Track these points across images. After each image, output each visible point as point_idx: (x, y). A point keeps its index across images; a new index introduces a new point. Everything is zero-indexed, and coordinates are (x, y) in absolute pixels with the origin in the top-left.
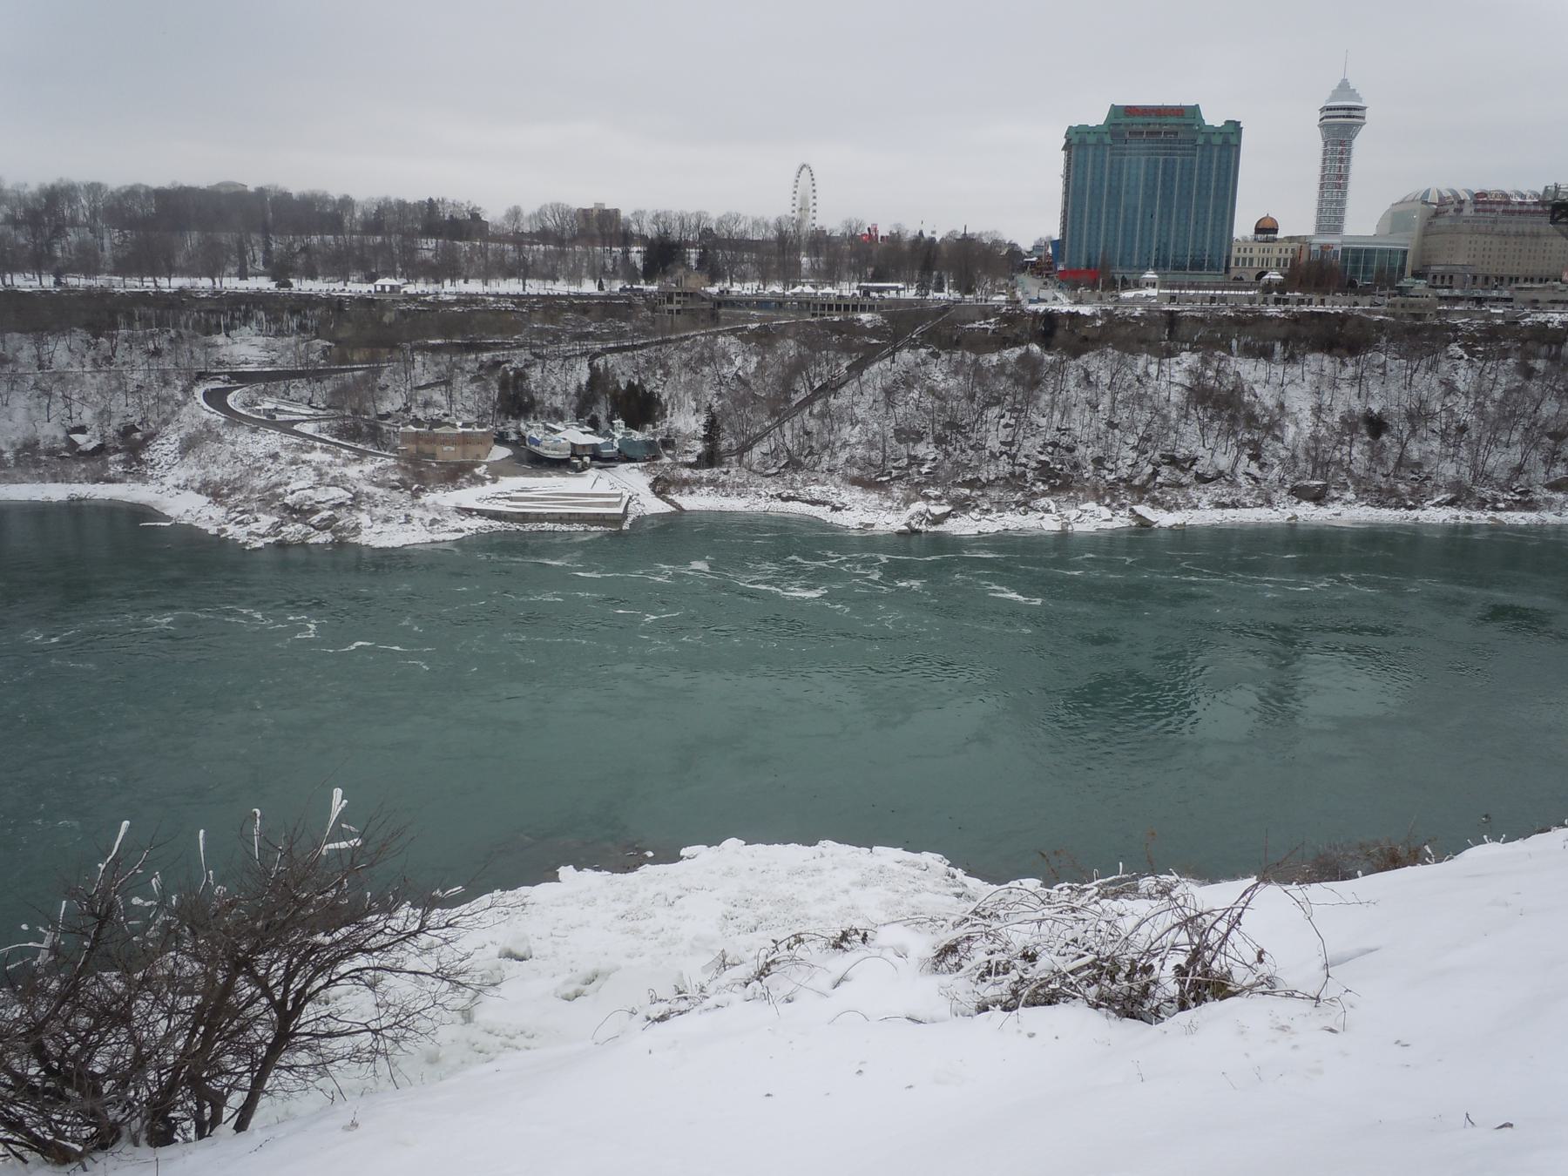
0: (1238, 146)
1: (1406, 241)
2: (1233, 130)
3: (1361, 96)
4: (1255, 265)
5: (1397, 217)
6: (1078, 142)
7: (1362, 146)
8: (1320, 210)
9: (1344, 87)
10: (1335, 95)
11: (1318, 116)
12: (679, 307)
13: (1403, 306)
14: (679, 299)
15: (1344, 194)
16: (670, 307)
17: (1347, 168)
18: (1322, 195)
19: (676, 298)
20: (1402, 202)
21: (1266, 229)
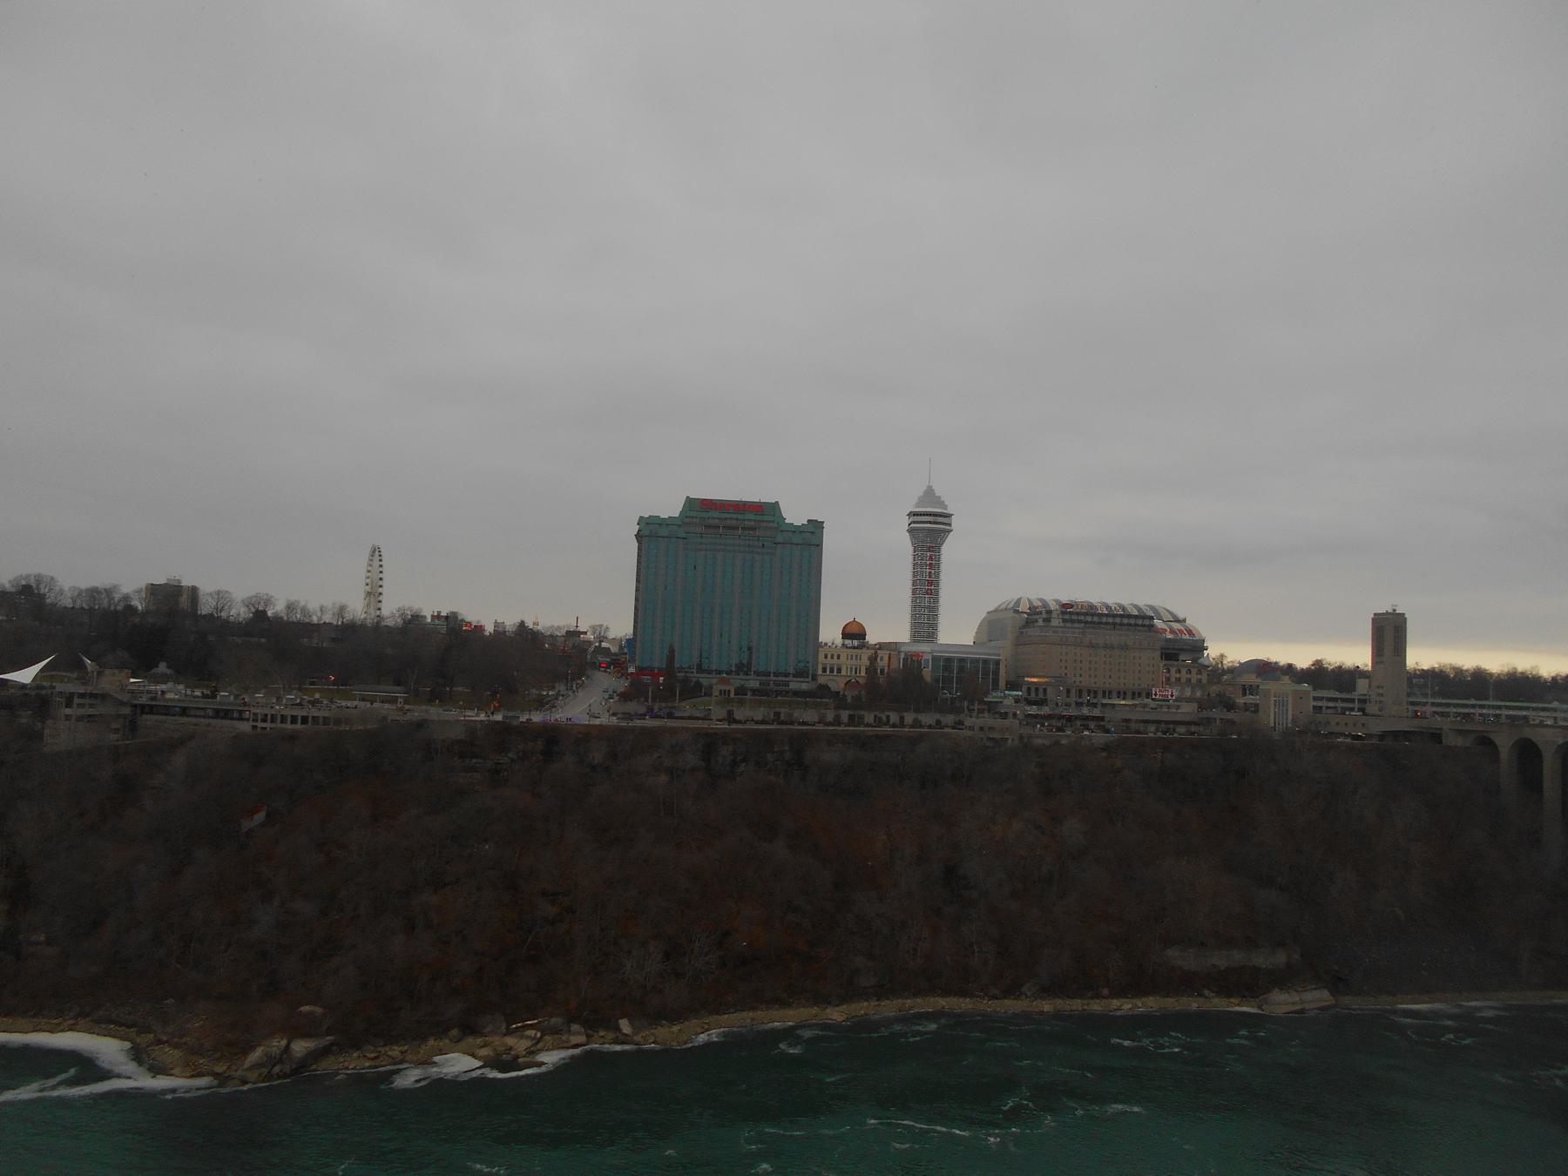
0: (819, 545)
1: (1001, 650)
2: (816, 527)
3: (946, 503)
4: (843, 673)
5: (992, 625)
6: (651, 533)
7: (951, 552)
8: (914, 617)
9: (930, 492)
10: (921, 502)
11: (906, 521)
12: (82, 711)
13: (981, 729)
14: (81, 701)
15: (936, 601)
16: (68, 711)
17: (938, 575)
18: (914, 600)
19: (76, 700)
20: (996, 611)
21: (854, 633)
